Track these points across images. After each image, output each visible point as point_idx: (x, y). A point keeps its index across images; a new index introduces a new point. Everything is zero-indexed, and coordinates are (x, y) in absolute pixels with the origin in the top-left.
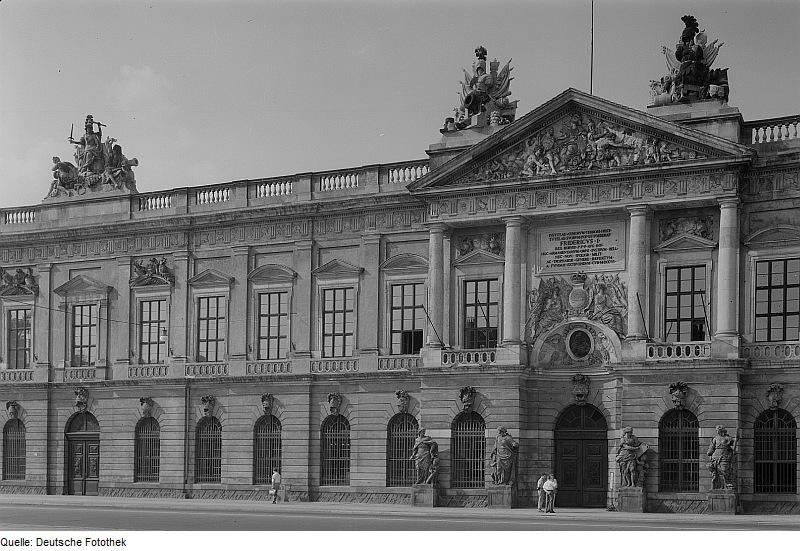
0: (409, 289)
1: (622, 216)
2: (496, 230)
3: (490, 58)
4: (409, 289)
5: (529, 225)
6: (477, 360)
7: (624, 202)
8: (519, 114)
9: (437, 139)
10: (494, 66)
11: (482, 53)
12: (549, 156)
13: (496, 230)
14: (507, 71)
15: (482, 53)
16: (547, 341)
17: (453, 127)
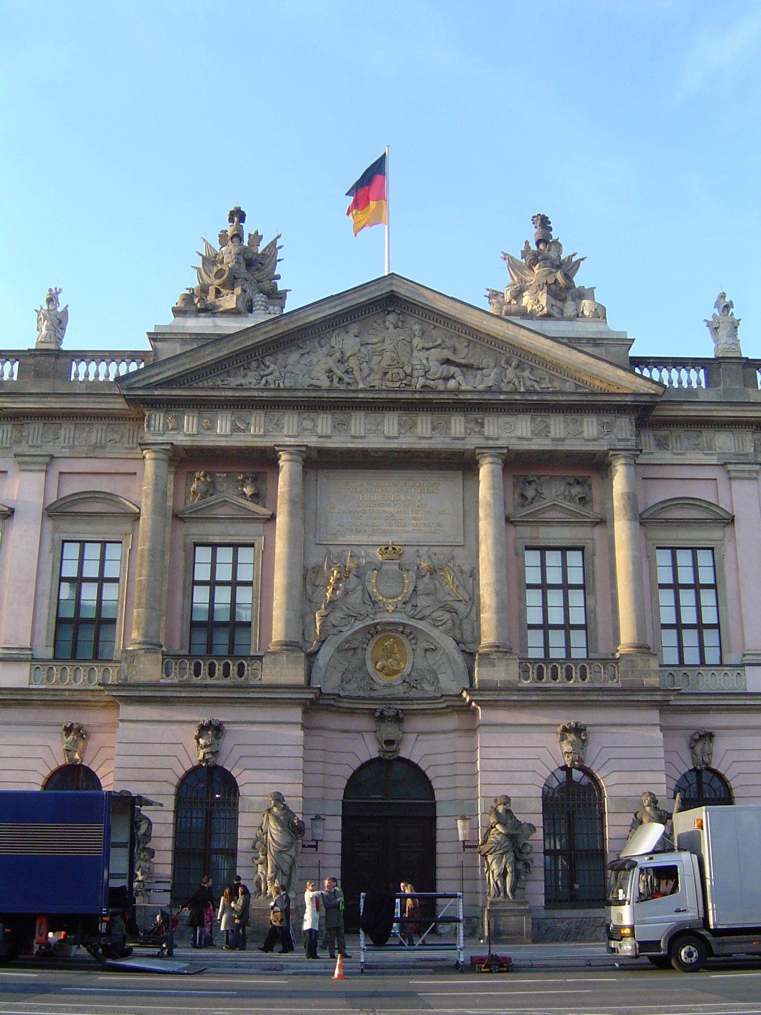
0: (92, 551)
1: (464, 464)
2: (262, 462)
3: (248, 228)
4: (92, 551)
5: (317, 462)
6: (226, 674)
7: (472, 443)
8: (290, 305)
9: (167, 319)
10: (256, 238)
11: (238, 216)
12: (353, 363)
13: (262, 462)
14: (273, 246)
15: (238, 216)
16: (339, 650)
17: (193, 304)
